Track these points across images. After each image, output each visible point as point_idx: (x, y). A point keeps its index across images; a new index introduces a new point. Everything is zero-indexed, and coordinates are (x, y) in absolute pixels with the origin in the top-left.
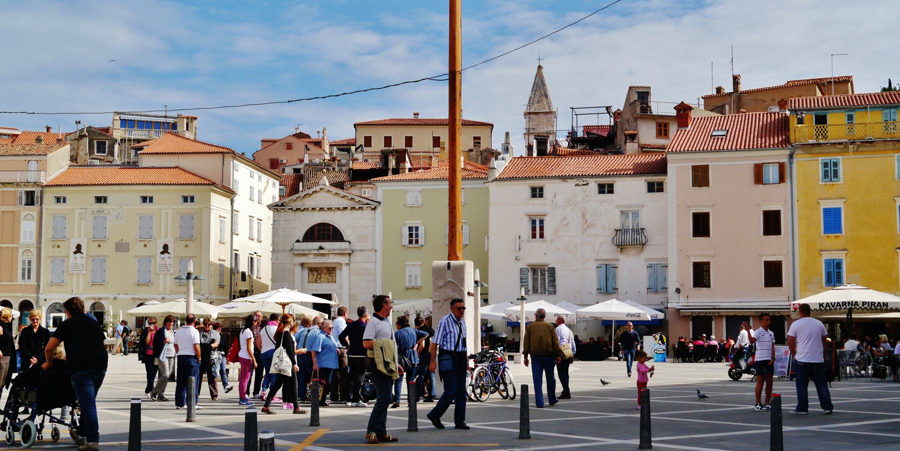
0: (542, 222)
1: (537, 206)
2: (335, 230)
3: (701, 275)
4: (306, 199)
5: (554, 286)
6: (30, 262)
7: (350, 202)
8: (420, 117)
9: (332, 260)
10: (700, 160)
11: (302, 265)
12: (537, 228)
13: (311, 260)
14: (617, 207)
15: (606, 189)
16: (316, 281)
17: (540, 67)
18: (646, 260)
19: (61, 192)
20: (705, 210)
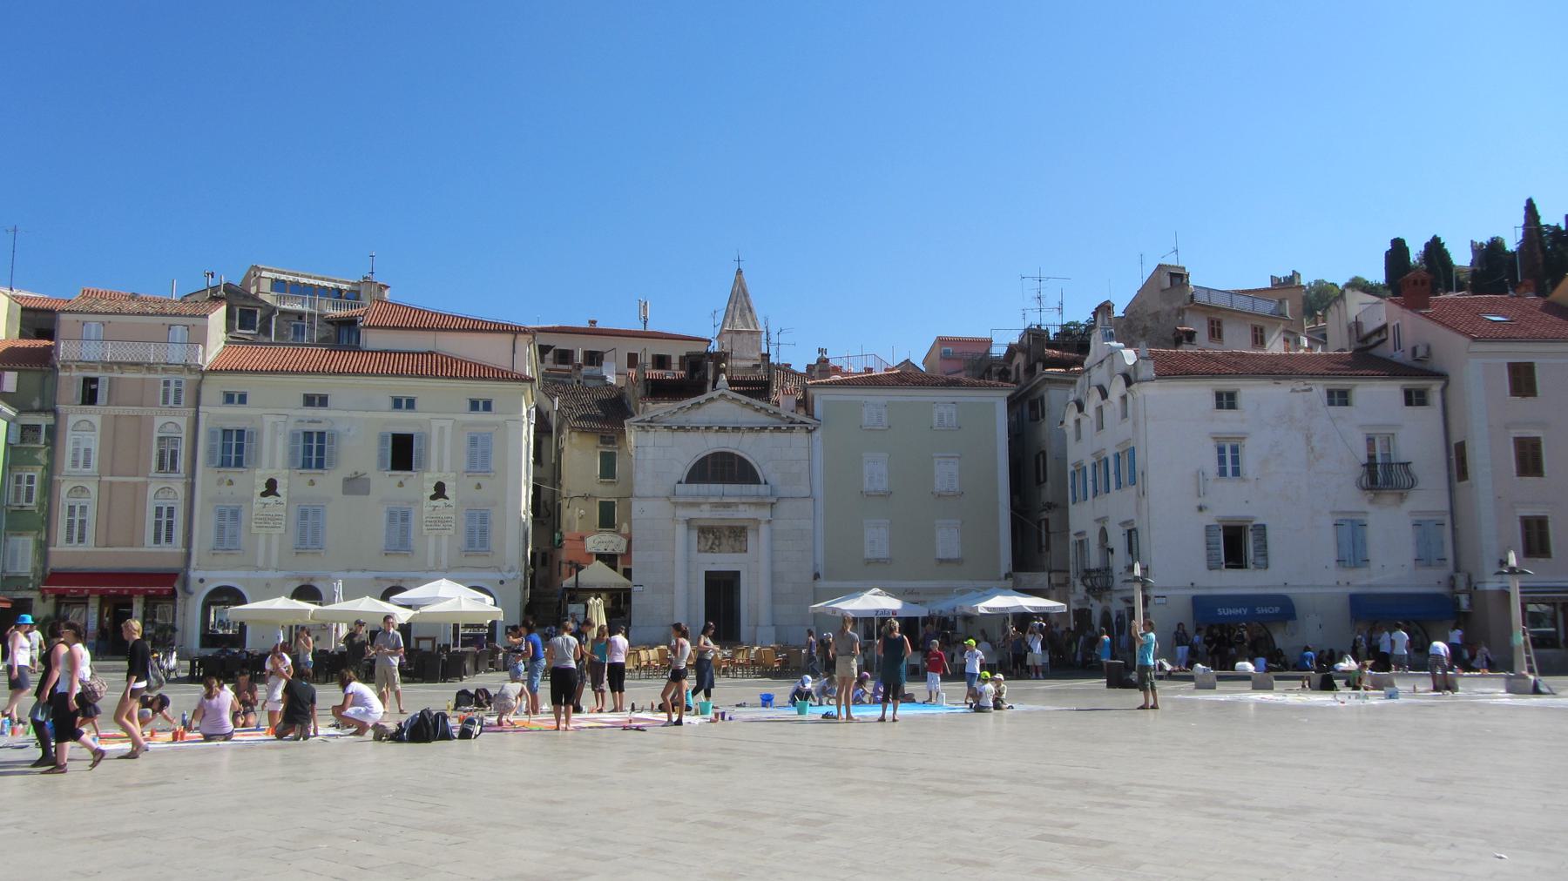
0: (1235, 450)
1: (1227, 422)
2: (743, 462)
3: (1235, 544)
4: (693, 412)
5: (1265, 556)
6: (171, 511)
7: (769, 419)
8: (599, 325)
9: (744, 513)
10: (1521, 352)
11: (689, 522)
12: (1229, 458)
13: (705, 514)
14: (1361, 426)
15: (1340, 398)
16: (711, 549)
17: (739, 272)
18: (1412, 513)
19: (236, 384)
20: (1533, 433)
